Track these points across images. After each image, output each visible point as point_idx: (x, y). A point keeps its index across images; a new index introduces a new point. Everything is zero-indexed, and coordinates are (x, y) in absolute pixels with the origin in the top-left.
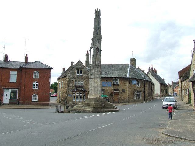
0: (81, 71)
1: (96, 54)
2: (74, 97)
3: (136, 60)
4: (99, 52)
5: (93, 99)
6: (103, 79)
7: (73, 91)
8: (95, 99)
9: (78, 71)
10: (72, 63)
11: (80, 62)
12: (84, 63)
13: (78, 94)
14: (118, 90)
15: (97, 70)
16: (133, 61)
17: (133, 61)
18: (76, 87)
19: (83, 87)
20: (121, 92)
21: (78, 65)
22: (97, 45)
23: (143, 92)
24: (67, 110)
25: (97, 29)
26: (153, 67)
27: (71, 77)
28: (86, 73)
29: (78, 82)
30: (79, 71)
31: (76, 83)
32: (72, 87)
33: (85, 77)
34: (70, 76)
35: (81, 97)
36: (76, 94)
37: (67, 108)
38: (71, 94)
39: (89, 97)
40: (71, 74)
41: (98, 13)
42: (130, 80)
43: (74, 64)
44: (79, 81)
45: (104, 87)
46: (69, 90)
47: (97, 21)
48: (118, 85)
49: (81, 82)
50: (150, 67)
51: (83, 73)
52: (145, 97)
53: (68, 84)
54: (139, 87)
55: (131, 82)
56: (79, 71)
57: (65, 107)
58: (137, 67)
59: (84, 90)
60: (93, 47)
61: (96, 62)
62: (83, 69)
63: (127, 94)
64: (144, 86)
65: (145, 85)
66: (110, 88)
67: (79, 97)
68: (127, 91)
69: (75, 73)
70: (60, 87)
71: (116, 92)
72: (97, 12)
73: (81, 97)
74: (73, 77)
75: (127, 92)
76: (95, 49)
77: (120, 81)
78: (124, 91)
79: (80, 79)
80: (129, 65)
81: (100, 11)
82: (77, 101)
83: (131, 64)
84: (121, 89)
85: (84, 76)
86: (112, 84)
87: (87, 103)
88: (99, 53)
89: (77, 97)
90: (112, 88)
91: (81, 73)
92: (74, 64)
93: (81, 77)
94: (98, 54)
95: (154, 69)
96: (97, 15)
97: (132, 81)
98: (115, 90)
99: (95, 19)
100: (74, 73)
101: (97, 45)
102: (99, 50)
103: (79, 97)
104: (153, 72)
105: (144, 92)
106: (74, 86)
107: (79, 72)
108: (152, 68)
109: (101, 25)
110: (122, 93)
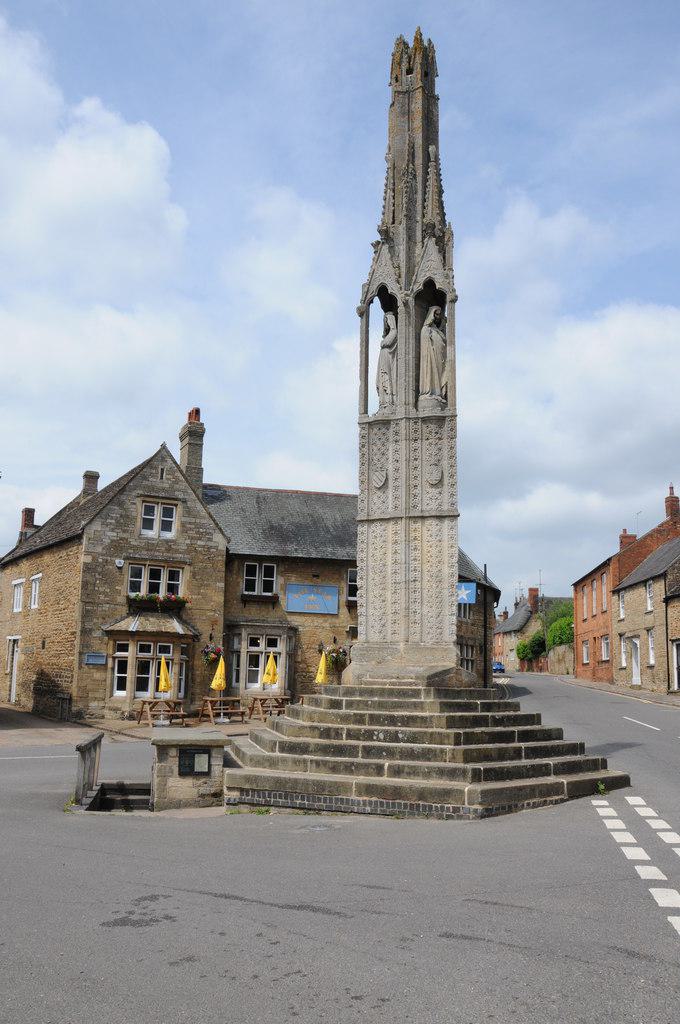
0: (168, 513)
10: (91, 478)
13: (144, 649)
24: (189, 782)
27: (108, 548)
28: (198, 526)
37: (187, 770)
41: (416, 66)
43: (102, 485)
51: (183, 525)
53: (85, 584)
54: (467, 623)
57: (173, 762)
61: (417, 392)
74: (117, 547)
92: (102, 485)
93: (169, 550)
100: (124, 522)
107: (158, 516)
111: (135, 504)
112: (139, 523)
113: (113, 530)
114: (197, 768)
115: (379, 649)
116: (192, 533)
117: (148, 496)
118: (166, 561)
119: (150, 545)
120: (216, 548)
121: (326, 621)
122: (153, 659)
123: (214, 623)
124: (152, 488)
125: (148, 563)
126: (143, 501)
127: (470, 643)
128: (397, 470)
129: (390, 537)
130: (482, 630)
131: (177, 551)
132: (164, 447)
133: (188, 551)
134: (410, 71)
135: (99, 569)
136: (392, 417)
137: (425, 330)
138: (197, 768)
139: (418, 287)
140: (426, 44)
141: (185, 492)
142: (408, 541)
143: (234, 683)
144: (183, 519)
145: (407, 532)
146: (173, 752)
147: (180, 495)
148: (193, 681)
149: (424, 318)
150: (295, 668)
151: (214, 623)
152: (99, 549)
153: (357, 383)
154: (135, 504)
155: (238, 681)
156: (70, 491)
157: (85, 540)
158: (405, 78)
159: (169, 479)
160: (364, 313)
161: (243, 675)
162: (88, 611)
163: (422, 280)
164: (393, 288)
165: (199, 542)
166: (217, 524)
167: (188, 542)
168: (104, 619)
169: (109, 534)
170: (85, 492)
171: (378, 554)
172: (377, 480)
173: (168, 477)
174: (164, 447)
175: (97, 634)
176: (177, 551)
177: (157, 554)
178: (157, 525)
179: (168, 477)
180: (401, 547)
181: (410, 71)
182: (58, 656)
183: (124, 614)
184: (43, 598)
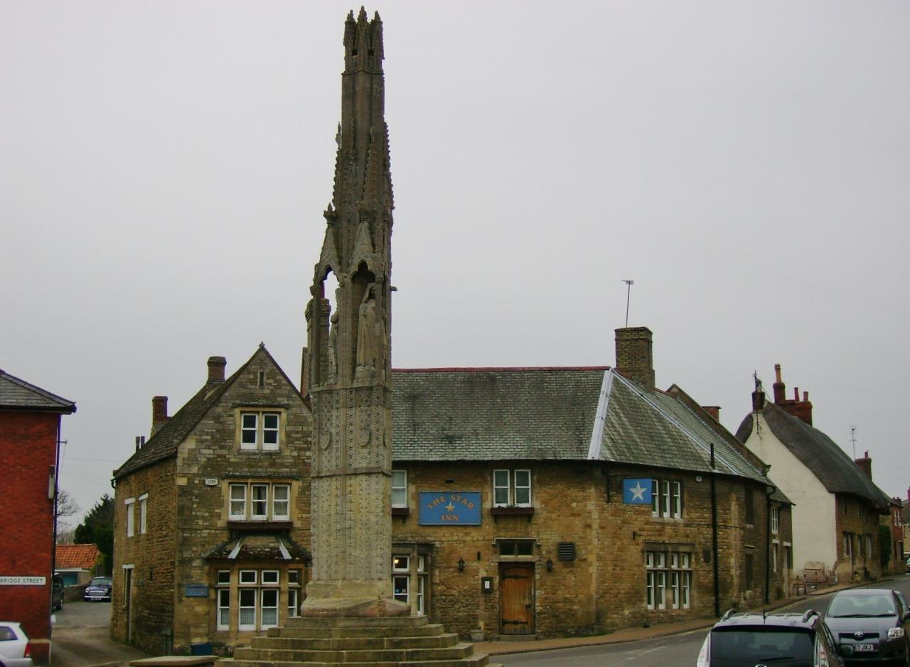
0: (271, 422)
1: (356, 315)
2: (225, 601)
3: (654, 338)
4: (372, 296)
5: (333, 615)
6: (417, 470)
7: (218, 563)
8: (351, 613)
9: (250, 422)
10: (216, 364)
11: (262, 356)
12: (293, 370)
14: (526, 547)
15: (358, 416)
16: (634, 345)
17: (634, 345)
18: (239, 531)
19: (282, 531)
20: (550, 562)
21: (253, 382)
22: (362, 250)
23: (707, 561)
25: (362, 143)
26: (783, 380)
27: (204, 467)
29: (249, 496)
30: (260, 421)
31: (237, 507)
32: (206, 535)
34: (192, 459)
35: (270, 598)
36: (236, 582)
38: (205, 582)
40: (200, 441)
41: (364, 40)
42: (609, 476)
44: (260, 492)
45: (429, 531)
46: (187, 555)
47: (358, 89)
48: (528, 515)
49: (270, 497)
50: (758, 383)
51: (288, 435)
52: (717, 588)
54: (675, 524)
55: (620, 489)
56: (260, 421)
58: (662, 383)
59: (295, 551)
60: (333, 264)
61: (354, 364)
62: (287, 407)
63: (593, 570)
64: (708, 515)
65: (719, 510)
66: (475, 535)
67: (258, 599)
68: (593, 549)
69: (232, 434)
70: (131, 534)
71: (517, 565)
72: (362, 34)
73: (270, 598)
74: (215, 467)
75: (592, 558)
76: (348, 280)
77: (540, 483)
78: (568, 553)
79: (265, 476)
80: (607, 379)
81: (377, 22)
82: (243, 628)
83: (619, 369)
84: (547, 536)
85: (290, 454)
86: (487, 505)
87: (295, 644)
88: (372, 304)
89: (247, 597)
90: (489, 532)
91: (270, 438)
94: (369, 307)
95: (790, 396)
96: (362, 52)
97: (626, 482)
98: (505, 547)
99: (349, 77)
100: (222, 437)
101: (362, 250)
102: (377, 287)
103: (258, 599)
104: (787, 414)
105: (712, 555)
106: (221, 523)
107: (260, 426)
108: (779, 388)
109: (387, 118)
110: (557, 566)
111: (232, 416)
112: (239, 436)
113: (209, 448)
117: (247, 406)
118: (269, 477)
121: (467, 534)
122: (257, 588)
124: (251, 396)
125: (250, 481)
126: (242, 412)
127: (687, 549)
130: (708, 532)
131: (283, 465)
132: (262, 347)
133: (294, 465)
135: (196, 492)
139: (354, 268)
140: (370, 18)
141: (289, 397)
142: (344, 495)
144: (288, 428)
149: (363, 294)
150: (433, 591)
152: (195, 470)
154: (232, 416)
156: (199, 379)
157: (179, 462)
159: (270, 384)
162: (185, 539)
163: (356, 262)
167: (295, 453)
168: (203, 546)
169: (205, 451)
170: (210, 382)
171: (325, 505)
173: (271, 381)
174: (262, 347)
175: (197, 563)
176: (283, 465)
177: (260, 470)
178: (260, 437)
180: (339, 500)
182: (162, 588)
183: (225, 540)
184: (149, 527)
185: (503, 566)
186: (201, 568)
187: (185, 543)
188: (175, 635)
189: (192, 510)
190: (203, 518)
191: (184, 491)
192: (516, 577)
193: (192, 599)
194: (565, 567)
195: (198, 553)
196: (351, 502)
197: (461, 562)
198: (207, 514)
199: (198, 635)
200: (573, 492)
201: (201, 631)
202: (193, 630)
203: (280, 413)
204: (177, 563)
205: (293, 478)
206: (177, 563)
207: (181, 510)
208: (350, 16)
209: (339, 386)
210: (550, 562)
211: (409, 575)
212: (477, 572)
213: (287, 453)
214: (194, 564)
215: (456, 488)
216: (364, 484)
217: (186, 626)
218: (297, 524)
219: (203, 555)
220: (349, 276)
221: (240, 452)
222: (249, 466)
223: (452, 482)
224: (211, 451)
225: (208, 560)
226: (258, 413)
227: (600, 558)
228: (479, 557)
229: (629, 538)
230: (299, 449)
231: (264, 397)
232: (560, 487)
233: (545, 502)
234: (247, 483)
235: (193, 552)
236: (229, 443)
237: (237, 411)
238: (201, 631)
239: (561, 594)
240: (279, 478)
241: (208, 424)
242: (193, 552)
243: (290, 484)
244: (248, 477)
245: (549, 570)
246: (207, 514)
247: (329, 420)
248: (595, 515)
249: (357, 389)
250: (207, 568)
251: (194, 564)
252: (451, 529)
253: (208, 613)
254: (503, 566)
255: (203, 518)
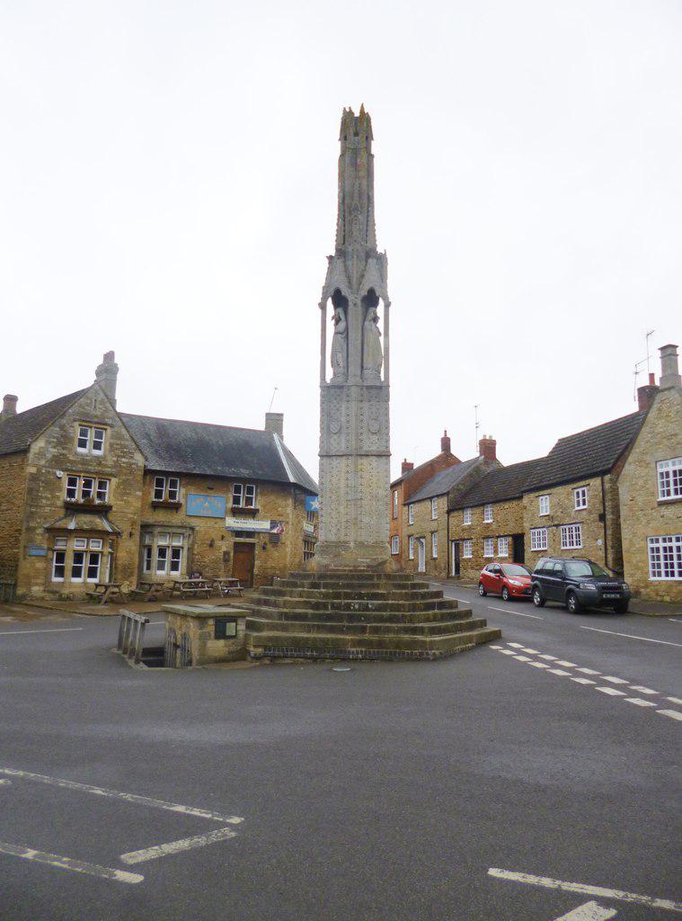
0: (99, 435)
9: (84, 433)
24: (221, 643)
33: (116, 465)
34: (41, 454)
37: (220, 634)
38: (45, 546)
39: (412, 557)
40: (48, 442)
41: (356, 130)
45: (193, 520)
46: (32, 524)
51: (111, 445)
62: (112, 426)
71: (245, 544)
74: (58, 461)
75: (288, 543)
85: (111, 460)
91: (97, 446)
92: (21, 408)
93: (100, 464)
100: (64, 440)
114: (228, 633)
115: (336, 547)
116: (118, 452)
117: (83, 421)
119: (84, 461)
120: (136, 464)
122: (86, 552)
123: (133, 523)
124: (87, 415)
125: (82, 474)
128: (348, 421)
129: (344, 469)
131: (106, 466)
133: (114, 467)
134: (356, 134)
135: (43, 479)
136: (345, 384)
137: (367, 323)
138: (228, 633)
139: (364, 292)
142: (356, 472)
143: (145, 571)
144: (112, 441)
145: (356, 466)
146: (211, 622)
147: (109, 422)
148: (116, 568)
150: (193, 559)
151: (133, 523)
152: (43, 462)
153: (320, 357)
155: (148, 568)
157: (31, 455)
158: (351, 137)
160: (323, 306)
161: (154, 564)
162: (32, 512)
164: (345, 292)
165: (124, 460)
166: (137, 446)
167: (115, 459)
169: (51, 449)
172: (334, 427)
173: (101, 406)
175: (40, 531)
179: (101, 406)
181: (356, 134)
183: (62, 516)
185: (236, 544)
186: (42, 535)
187: (31, 516)
188: (19, 584)
189: (38, 491)
190: (47, 498)
191: (34, 478)
192: (242, 552)
193: (33, 558)
194: (273, 547)
195: (40, 526)
196: (361, 477)
197: (213, 541)
198: (49, 496)
199: (37, 584)
200: (280, 501)
201: (39, 581)
202: (33, 581)
203: (106, 429)
204: (24, 531)
205: (112, 475)
206: (24, 531)
207: (30, 491)
208: (345, 109)
209: (349, 383)
210: (265, 544)
211: (182, 548)
212: (220, 547)
213: (109, 458)
214: (37, 532)
215: (212, 493)
216: (374, 464)
217: (27, 576)
218: (114, 509)
219: (45, 526)
220: (360, 298)
221: (76, 454)
222: (82, 464)
223: (212, 489)
224: (56, 450)
225: (49, 530)
226: (91, 427)
227: (291, 544)
228: (223, 537)
229: (594, 521)
230: (119, 456)
231: (96, 416)
232: (273, 497)
233: (264, 506)
234: (79, 476)
235: (37, 523)
236: (69, 446)
237: (76, 424)
238: (39, 581)
239: (269, 564)
240: (103, 474)
241: (55, 430)
242: (37, 523)
243: (110, 480)
244: (81, 472)
245: (264, 548)
246: (49, 496)
247: (338, 410)
248: (290, 516)
249: (368, 387)
250: (47, 535)
251: (37, 532)
252: (207, 519)
253: (45, 569)
254: (236, 544)
255: (47, 498)
